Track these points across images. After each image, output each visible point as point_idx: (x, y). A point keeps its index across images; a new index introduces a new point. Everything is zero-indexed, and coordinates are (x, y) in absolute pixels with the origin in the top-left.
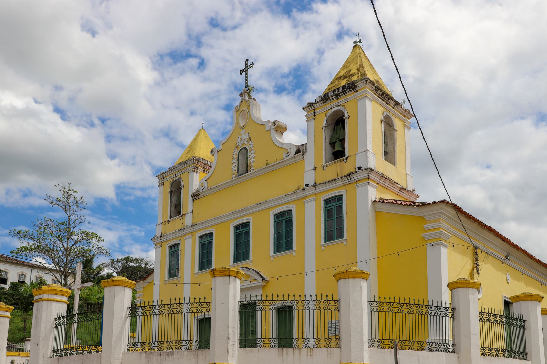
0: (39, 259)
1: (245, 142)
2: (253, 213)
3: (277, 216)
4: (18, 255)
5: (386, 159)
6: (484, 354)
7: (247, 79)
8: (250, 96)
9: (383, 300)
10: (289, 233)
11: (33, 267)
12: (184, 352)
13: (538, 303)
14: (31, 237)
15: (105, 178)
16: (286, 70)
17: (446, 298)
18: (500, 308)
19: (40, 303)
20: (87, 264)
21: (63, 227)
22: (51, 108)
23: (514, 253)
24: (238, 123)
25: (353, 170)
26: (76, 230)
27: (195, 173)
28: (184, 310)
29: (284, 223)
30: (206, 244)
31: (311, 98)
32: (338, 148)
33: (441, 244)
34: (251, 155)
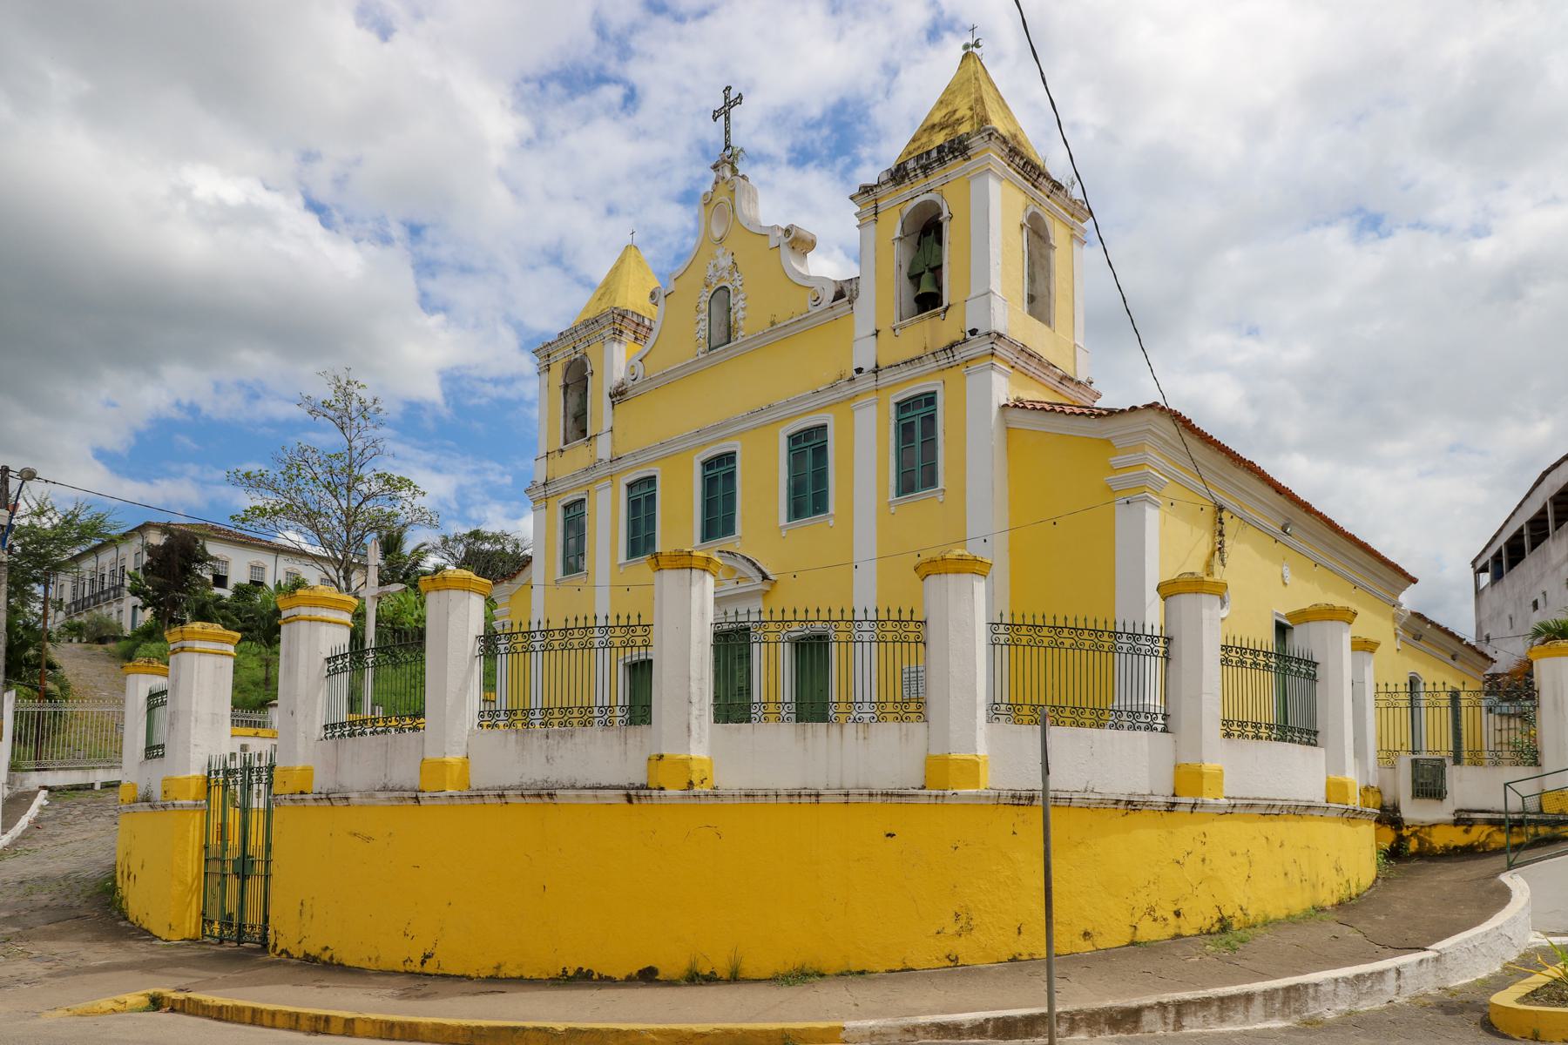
0: (291, 535)
1: (725, 274)
3: (794, 439)
4: (247, 525)
5: (1031, 313)
6: (1228, 735)
7: (727, 132)
8: (734, 171)
9: (1018, 621)
10: (821, 477)
11: (279, 550)
12: (596, 731)
13: (1344, 625)
14: (272, 487)
15: (420, 356)
16: (815, 111)
17: (1153, 615)
18: (1268, 639)
19: (294, 626)
20: (391, 545)
21: (337, 465)
22: (299, 200)
23: (1303, 522)
24: (708, 232)
25: (960, 337)
26: (367, 472)
27: (616, 345)
28: (596, 642)
29: (809, 449)
30: (642, 499)
31: (869, 174)
32: (927, 287)
33: (1146, 499)
34: (737, 302)
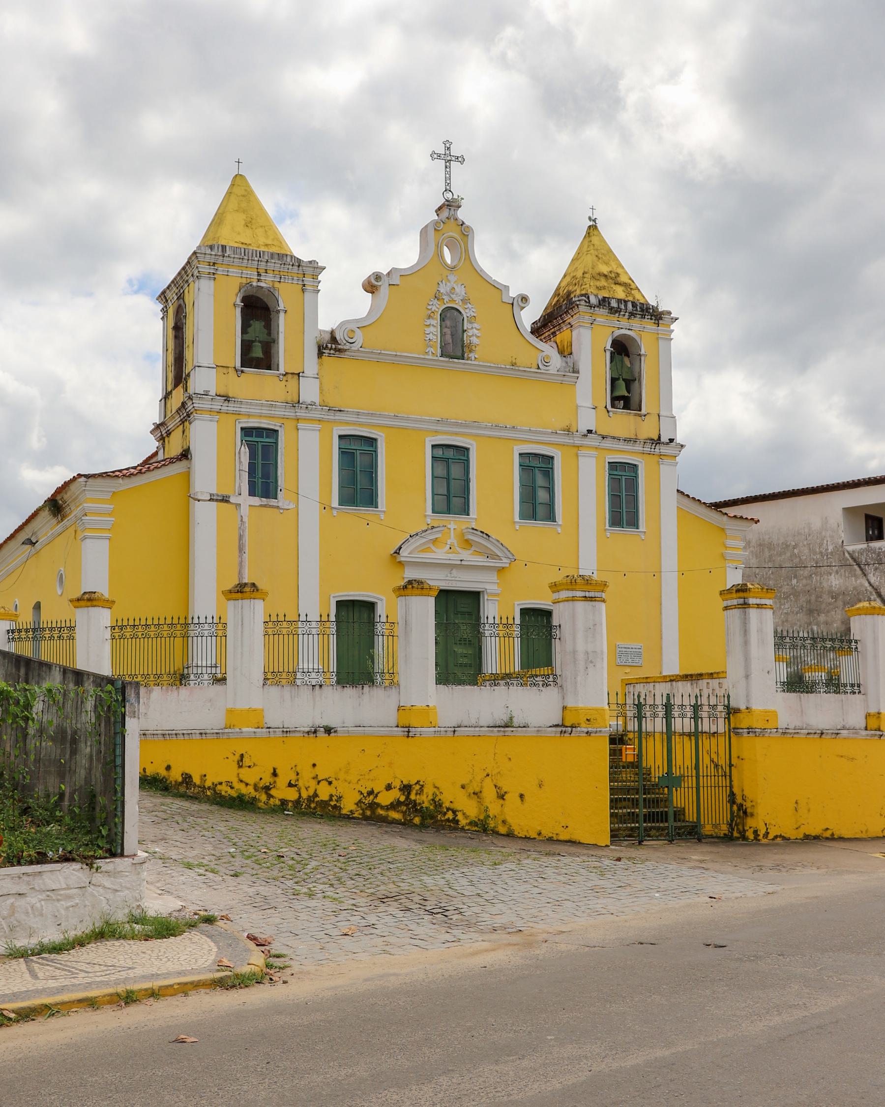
2: (477, 435)
32: (622, 392)
